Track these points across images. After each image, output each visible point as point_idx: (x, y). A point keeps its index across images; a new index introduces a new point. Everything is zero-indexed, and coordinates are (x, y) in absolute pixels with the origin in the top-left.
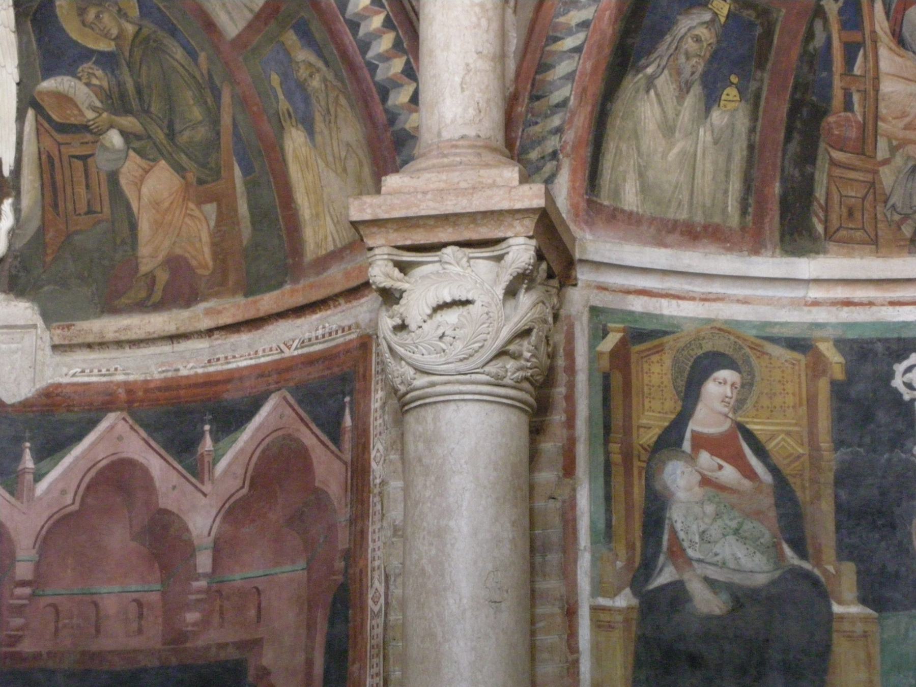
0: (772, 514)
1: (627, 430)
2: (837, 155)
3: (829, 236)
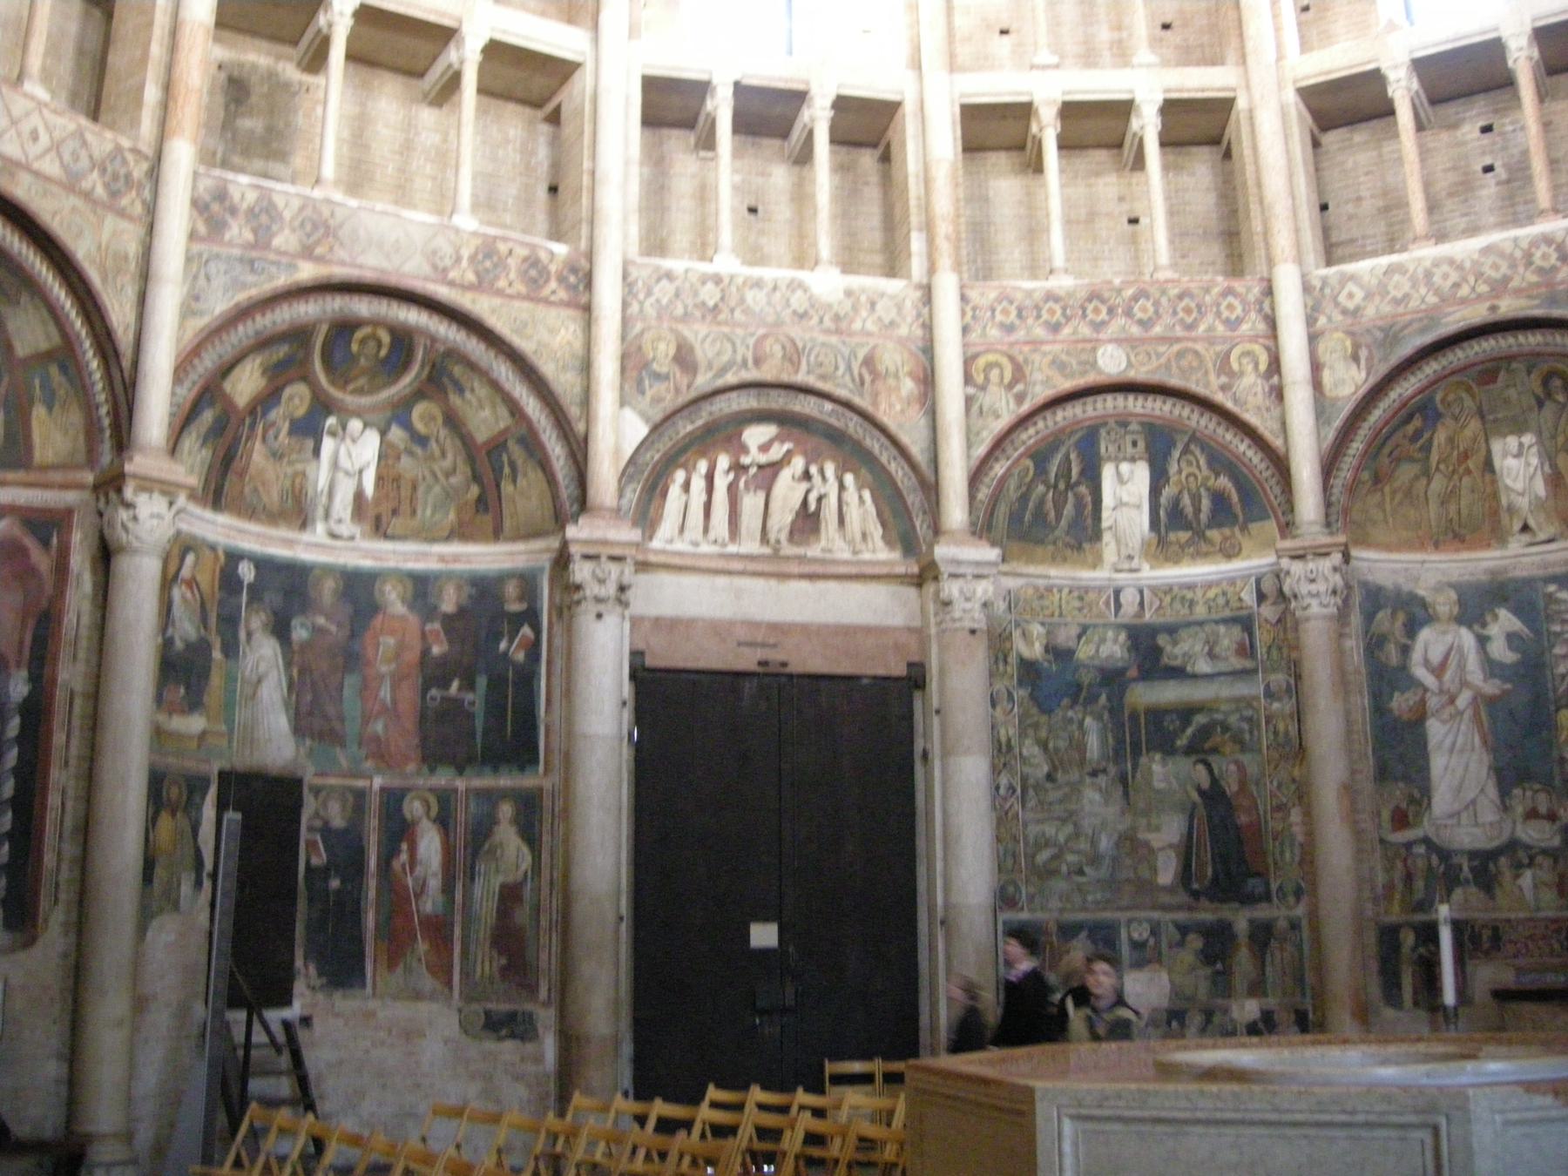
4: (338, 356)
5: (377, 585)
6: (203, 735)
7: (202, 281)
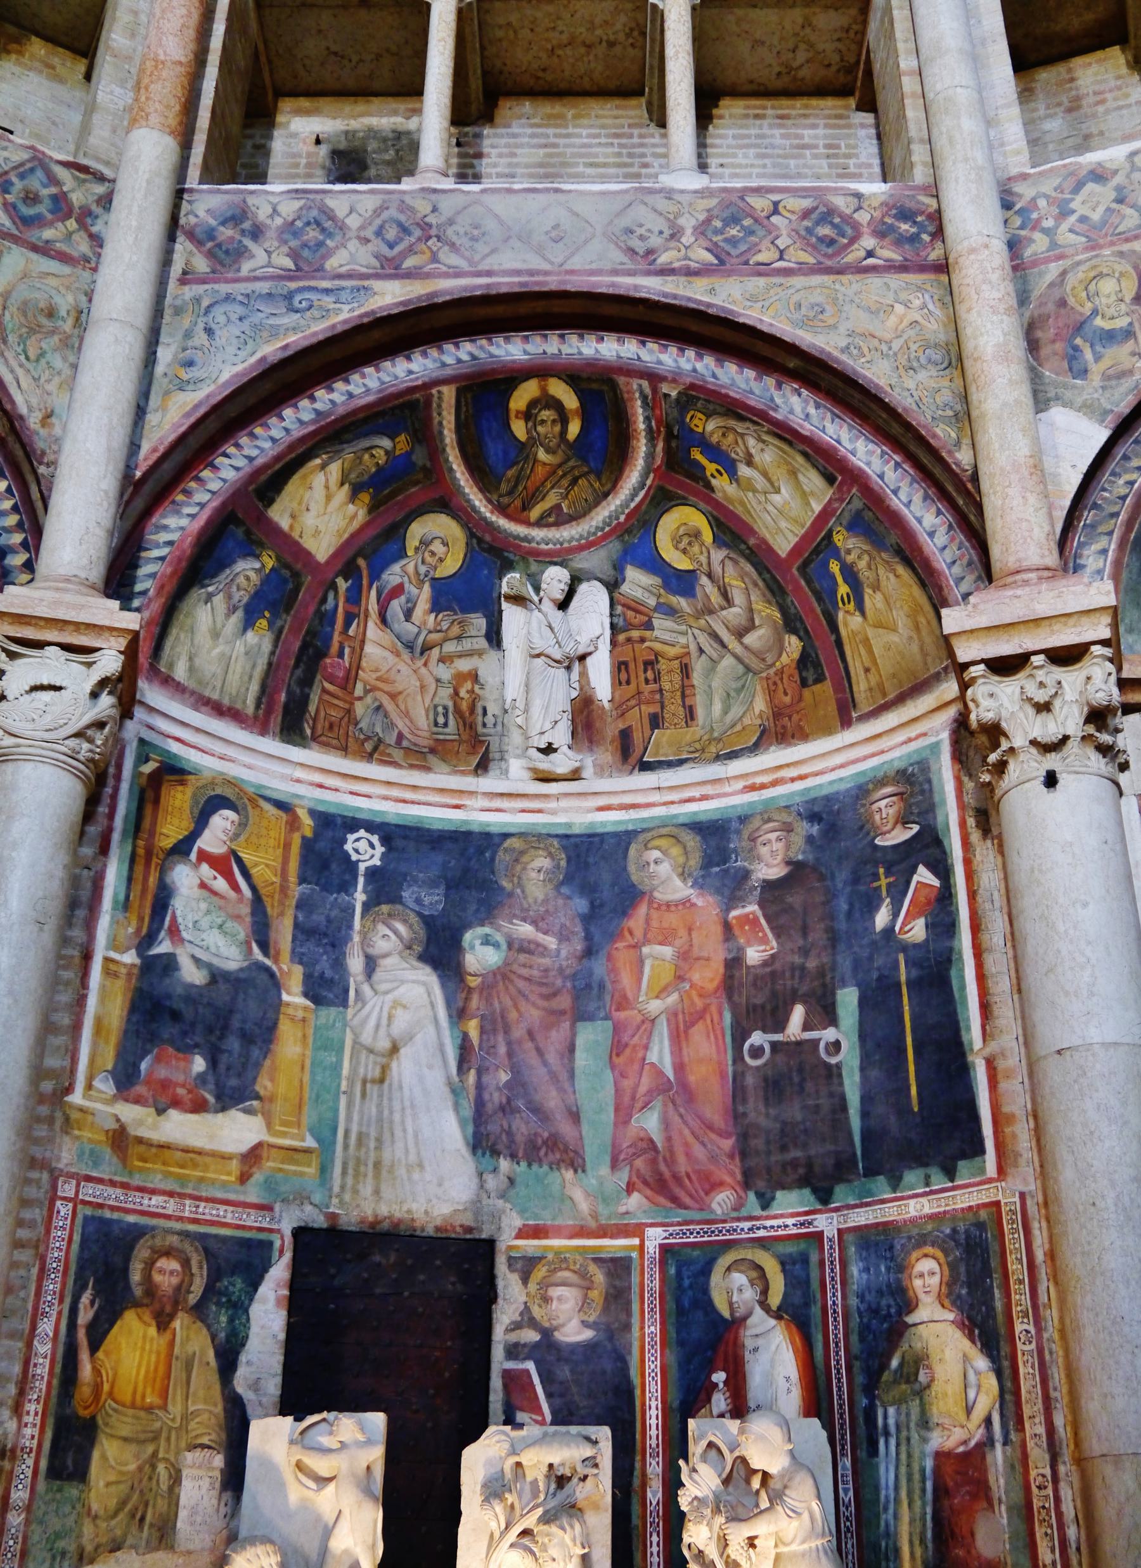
0: (248, 919)
1: (152, 833)
2: (327, 685)
3: (314, 738)
4: (494, 450)
5: (632, 852)
6: (253, 1156)
7: (201, 338)
